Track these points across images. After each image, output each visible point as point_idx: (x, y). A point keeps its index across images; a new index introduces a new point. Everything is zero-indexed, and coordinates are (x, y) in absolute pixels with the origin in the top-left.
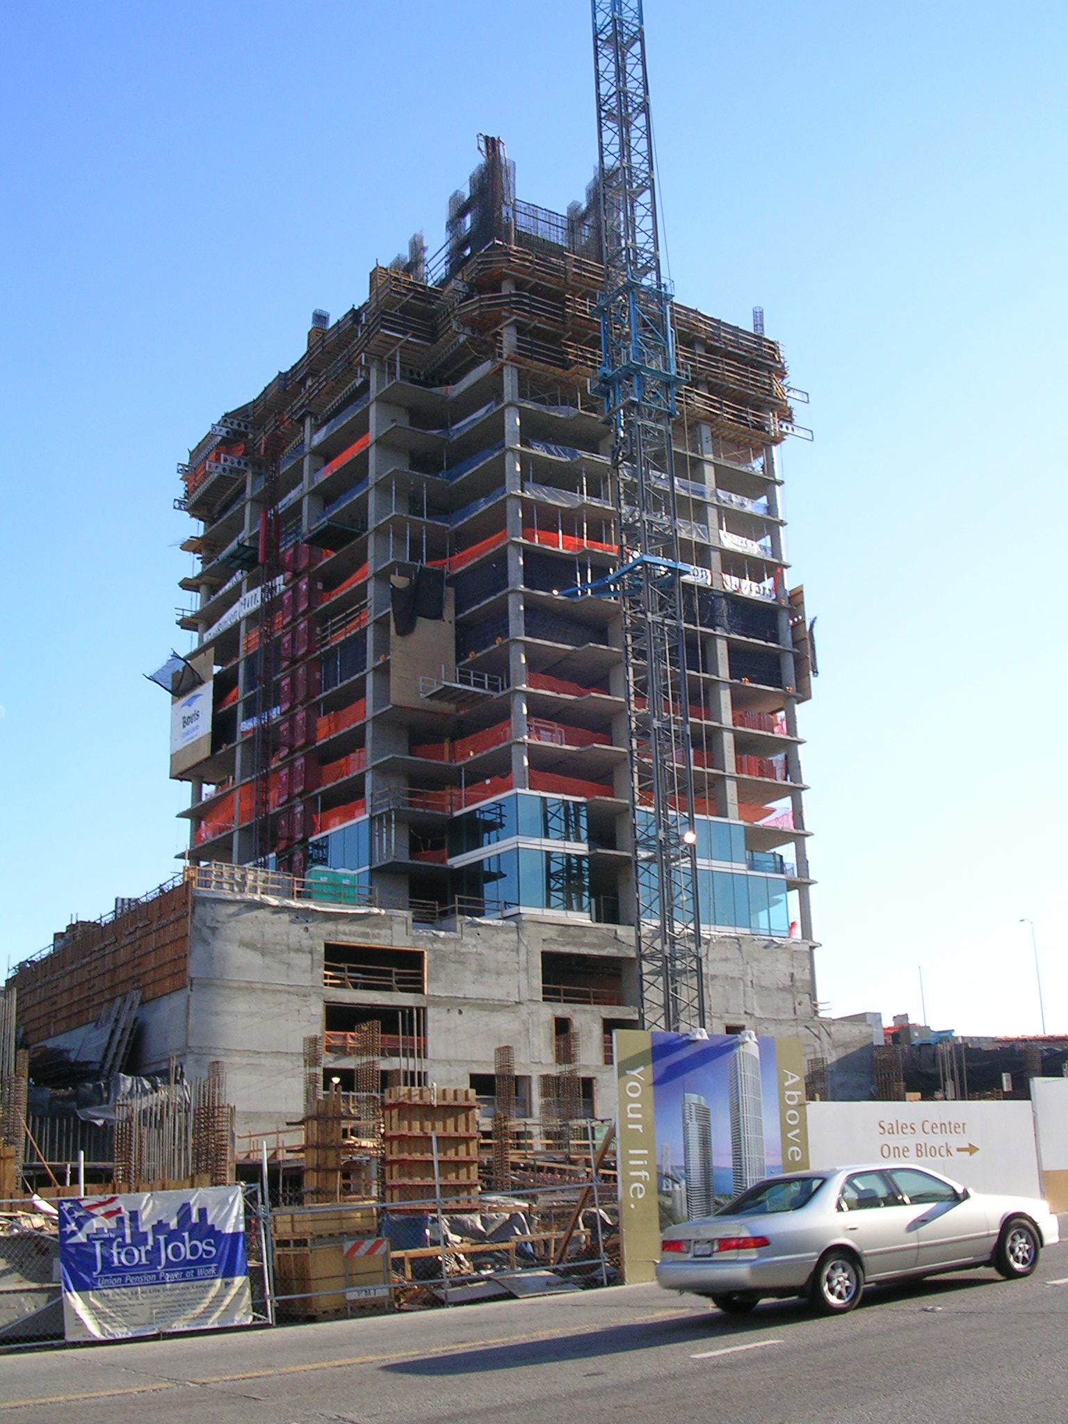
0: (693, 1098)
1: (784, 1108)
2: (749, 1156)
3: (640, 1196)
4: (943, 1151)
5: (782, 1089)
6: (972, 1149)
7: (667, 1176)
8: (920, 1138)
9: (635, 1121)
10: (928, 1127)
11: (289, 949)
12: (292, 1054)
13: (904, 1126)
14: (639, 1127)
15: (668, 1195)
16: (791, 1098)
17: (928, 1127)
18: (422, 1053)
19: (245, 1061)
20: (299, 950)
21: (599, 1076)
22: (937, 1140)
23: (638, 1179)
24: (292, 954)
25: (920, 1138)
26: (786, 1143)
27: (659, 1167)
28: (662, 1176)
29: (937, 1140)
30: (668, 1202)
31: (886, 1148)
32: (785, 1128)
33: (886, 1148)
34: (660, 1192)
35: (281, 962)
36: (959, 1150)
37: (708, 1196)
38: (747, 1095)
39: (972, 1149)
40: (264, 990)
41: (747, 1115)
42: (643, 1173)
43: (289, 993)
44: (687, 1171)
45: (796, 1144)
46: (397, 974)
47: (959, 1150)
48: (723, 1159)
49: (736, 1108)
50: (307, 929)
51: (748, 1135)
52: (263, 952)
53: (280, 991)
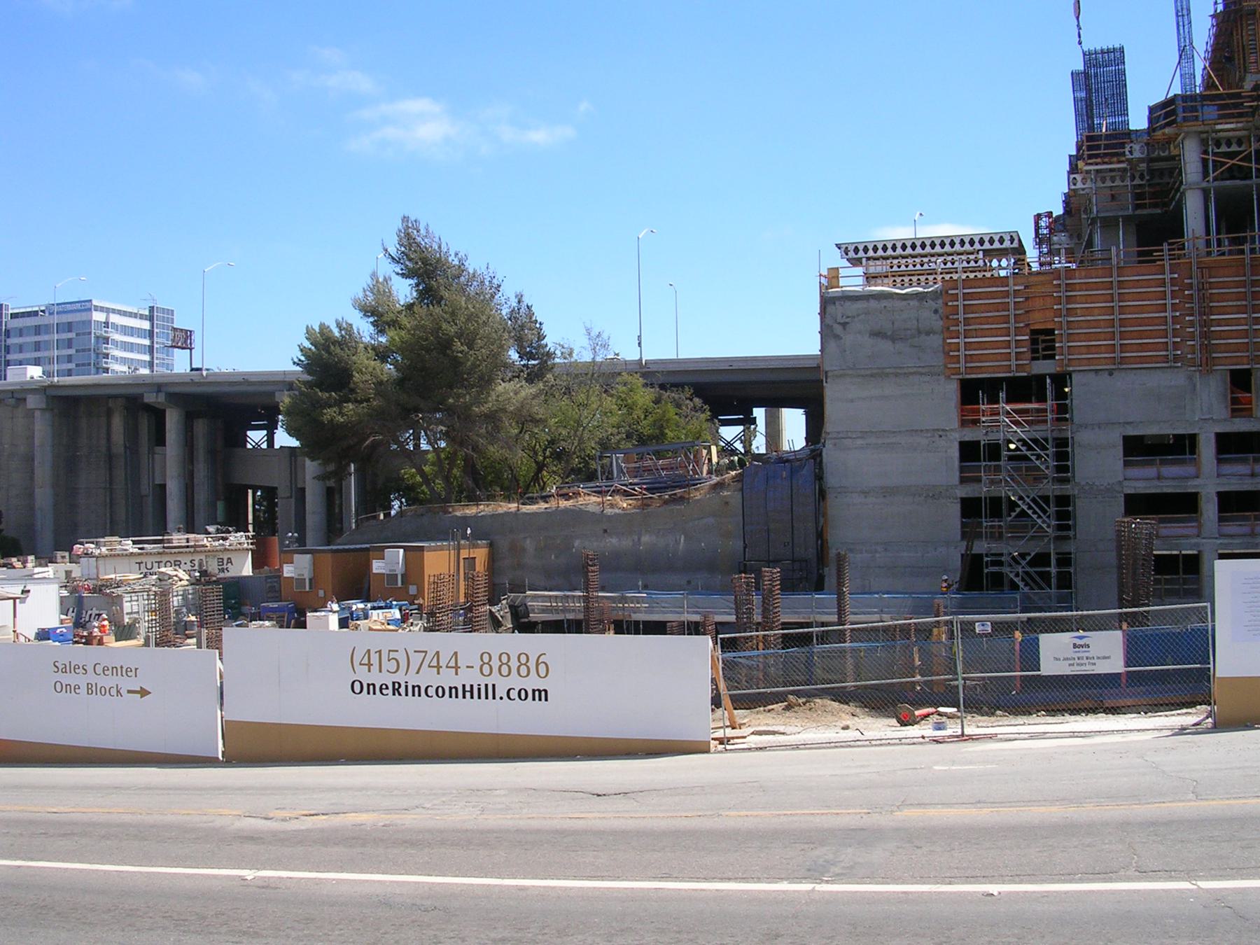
6: (143, 693)
10: (99, 669)
11: (919, 332)
13: (77, 667)
17: (99, 669)
19: (880, 441)
20: (928, 333)
24: (923, 337)
25: (92, 678)
31: (58, 685)
33: (58, 685)
35: (912, 346)
36: (129, 692)
39: (143, 693)
40: (896, 375)
43: (921, 374)
46: (1044, 341)
47: (129, 692)
50: (936, 311)
52: (893, 339)
53: (911, 374)
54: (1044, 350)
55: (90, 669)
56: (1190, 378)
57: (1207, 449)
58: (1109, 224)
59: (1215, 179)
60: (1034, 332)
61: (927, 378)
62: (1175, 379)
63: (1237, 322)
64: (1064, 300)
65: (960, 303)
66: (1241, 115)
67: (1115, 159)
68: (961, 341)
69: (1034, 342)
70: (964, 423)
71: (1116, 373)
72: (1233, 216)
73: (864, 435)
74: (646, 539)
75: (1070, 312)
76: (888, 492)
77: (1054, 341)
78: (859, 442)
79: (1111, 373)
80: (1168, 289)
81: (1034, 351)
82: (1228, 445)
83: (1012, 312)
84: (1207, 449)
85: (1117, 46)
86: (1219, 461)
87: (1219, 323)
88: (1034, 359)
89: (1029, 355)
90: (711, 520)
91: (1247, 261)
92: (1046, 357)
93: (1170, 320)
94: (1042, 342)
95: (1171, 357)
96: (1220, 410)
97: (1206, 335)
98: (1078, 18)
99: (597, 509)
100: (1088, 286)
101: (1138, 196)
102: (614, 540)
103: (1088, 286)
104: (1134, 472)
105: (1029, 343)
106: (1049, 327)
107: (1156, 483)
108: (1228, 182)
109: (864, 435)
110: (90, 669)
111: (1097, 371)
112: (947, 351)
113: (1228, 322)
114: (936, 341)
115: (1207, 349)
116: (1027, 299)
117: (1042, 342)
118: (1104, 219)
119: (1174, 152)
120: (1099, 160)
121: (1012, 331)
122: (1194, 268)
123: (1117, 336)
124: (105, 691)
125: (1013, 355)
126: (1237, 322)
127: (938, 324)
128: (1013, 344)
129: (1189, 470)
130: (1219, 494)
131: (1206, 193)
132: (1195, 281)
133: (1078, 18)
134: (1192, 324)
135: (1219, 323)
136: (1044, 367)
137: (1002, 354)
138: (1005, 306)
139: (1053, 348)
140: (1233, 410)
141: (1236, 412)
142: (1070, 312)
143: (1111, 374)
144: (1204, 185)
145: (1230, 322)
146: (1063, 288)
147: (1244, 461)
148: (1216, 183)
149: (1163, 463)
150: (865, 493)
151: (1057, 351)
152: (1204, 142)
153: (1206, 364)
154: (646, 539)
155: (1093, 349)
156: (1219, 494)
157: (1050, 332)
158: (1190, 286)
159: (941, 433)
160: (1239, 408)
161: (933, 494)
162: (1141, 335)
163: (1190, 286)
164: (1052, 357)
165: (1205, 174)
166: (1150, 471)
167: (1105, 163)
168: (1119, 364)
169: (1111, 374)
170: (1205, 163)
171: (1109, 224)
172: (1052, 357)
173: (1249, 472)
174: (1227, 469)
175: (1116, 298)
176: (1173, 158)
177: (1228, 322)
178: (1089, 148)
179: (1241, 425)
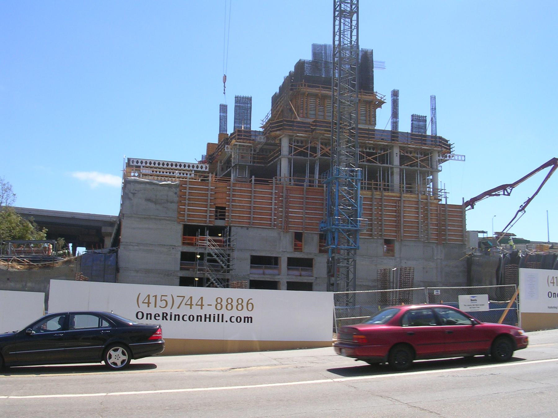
54: (220, 216)
57: (284, 264)
58: (242, 168)
59: (294, 155)
60: (217, 208)
61: (169, 222)
62: (273, 234)
63: (298, 213)
64: (231, 196)
65: (187, 191)
66: (306, 131)
67: (248, 141)
68: (187, 207)
69: (216, 212)
71: (250, 229)
72: (298, 170)
75: (234, 201)
77: (225, 212)
80: (274, 196)
81: (216, 216)
82: (293, 263)
83: (209, 198)
84: (284, 264)
85: (250, 96)
86: (288, 269)
87: (292, 212)
88: (216, 219)
89: (214, 217)
91: (305, 189)
92: (220, 219)
93: (273, 209)
94: (220, 212)
95: (272, 224)
97: (287, 217)
98: (224, 83)
100: (241, 191)
101: (254, 158)
103: (241, 191)
104: (254, 271)
105: (214, 212)
106: (224, 206)
108: (299, 157)
111: (242, 227)
112: (180, 212)
113: (295, 213)
114: (174, 206)
115: (287, 222)
116: (216, 193)
117: (220, 212)
118: (240, 165)
119: (277, 142)
120: (242, 141)
121: (209, 206)
122: (284, 189)
123: (252, 213)
125: (208, 216)
126: (298, 213)
127: (176, 199)
128: (208, 212)
129: (276, 272)
130: (288, 282)
131: (290, 160)
132: (284, 195)
133: (224, 83)
134: (282, 212)
135: (292, 212)
136: (220, 223)
137: (202, 215)
138: (206, 195)
139: (224, 215)
141: (296, 250)
142: (234, 201)
143: (247, 229)
144: (290, 156)
145: (296, 213)
146: (231, 190)
147: (297, 270)
148: (294, 157)
149: (266, 268)
151: (226, 217)
152: (290, 140)
153: (286, 229)
156: (288, 282)
157: (224, 208)
158: (282, 196)
162: (261, 214)
163: (282, 196)
164: (224, 219)
165: (290, 152)
166: (261, 271)
167: (243, 142)
168: (250, 225)
169: (247, 229)
170: (290, 147)
171: (242, 168)
172: (224, 219)
173: (299, 274)
174: (291, 272)
175: (253, 197)
176: (275, 145)
177: (295, 213)
178: (238, 135)
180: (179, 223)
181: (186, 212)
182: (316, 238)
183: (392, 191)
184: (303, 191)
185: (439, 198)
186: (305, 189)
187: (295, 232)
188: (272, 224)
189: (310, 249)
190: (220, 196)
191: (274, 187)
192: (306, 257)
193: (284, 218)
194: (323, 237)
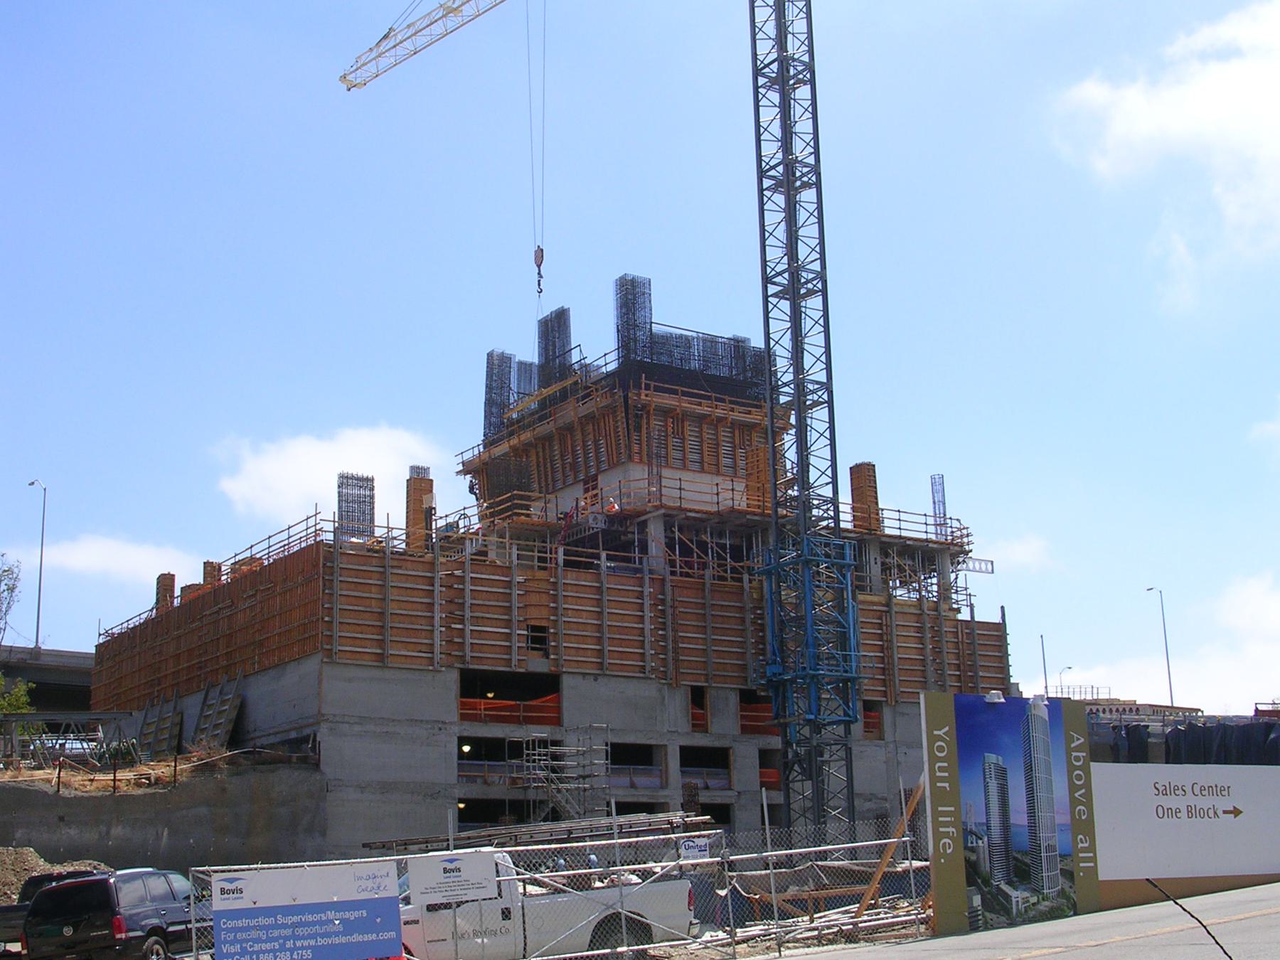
0: (992, 758)
1: (1071, 769)
2: (1043, 815)
3: (949, 851)
4: (1211, 813)
5: (1069, 751)
6: (1236, 812)
7: (972, 833)
8: (1191, 800)
9: (942, 779)
10: (1197, 791)
12: (427, 722)
13: (1176, 788)
14: (947, 785)
15: (973, 850)
16: (1077, 759)
17: (1197, 791)
18: (557, 722)
21: (735, 745)
22: (1204, 802)
23: (946, 835)
26: (1074, 802)
27: (965, 823)
28: (967, 833)
29: (1204, 802)
30: (973, 857)
31: (1160, 809)
32: (1073, 788)
33: (1160, 809)
34: (966, 848)
36: (1225, 812)
37: (1007, 851)
38: (1039, 756)
39: (1236, 812)
41: (1039, 774)
42: (951, 829)
44: (989, 828)
45: (1082, 803)
47: (1225, 812)
48: (1019, 817)
49: (1029, 770)
51: (1041, 795)
55: (1188, 789)
56: (660, 690)
62: (646, 691)
70: (464, 717)
71: (600, 679)
73: (362, 720)
74: (117, 831)
76: (386, 788)
78: (357, 728)
79: (596, 677)
90: (203, 810)
94: (539, 638)
96: (684, 725)
97: (676, 650)
99: (51, 790)
102: (73, 832)
106: (544, 624)
107: (633, 791)
109: (362, 720)
110: (1188, 789)
111: (584, 675)
117: (539, 638)
121: (515, 625)
124: (1203, 813)
132: (669, 598)
134: (664, 637)
140: (694, 725)
143: (596, 677)
150: (362, 788)
154: (117, 831)
155: (581, 652)
159: (442, 725)
160: (699, 724)
161: (432, 793)
168: (601, 670)
179: (700, 740)
180: (450, 666)
181: (469, 640)
182: (734, 699)
183: (871, 592)
184: (703, 590)
185: (955, 606)
186: (708, 585)
187: (692, 687)
188: (648, 668)
189: (724, 726)
190: (534, 599)
191: (647, 581)
192: (717, 744)
193: (670, 654)
194: (748, 698)
